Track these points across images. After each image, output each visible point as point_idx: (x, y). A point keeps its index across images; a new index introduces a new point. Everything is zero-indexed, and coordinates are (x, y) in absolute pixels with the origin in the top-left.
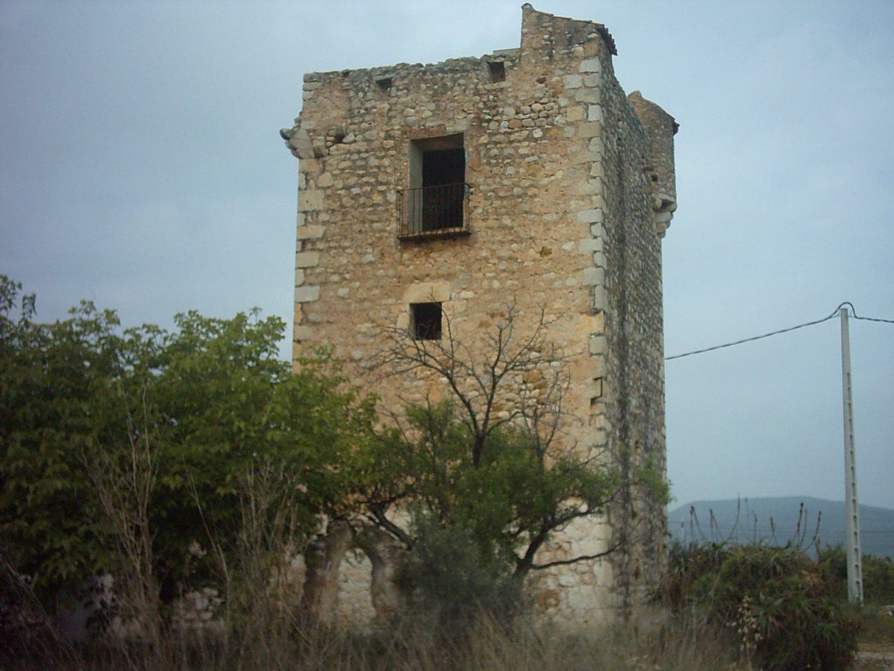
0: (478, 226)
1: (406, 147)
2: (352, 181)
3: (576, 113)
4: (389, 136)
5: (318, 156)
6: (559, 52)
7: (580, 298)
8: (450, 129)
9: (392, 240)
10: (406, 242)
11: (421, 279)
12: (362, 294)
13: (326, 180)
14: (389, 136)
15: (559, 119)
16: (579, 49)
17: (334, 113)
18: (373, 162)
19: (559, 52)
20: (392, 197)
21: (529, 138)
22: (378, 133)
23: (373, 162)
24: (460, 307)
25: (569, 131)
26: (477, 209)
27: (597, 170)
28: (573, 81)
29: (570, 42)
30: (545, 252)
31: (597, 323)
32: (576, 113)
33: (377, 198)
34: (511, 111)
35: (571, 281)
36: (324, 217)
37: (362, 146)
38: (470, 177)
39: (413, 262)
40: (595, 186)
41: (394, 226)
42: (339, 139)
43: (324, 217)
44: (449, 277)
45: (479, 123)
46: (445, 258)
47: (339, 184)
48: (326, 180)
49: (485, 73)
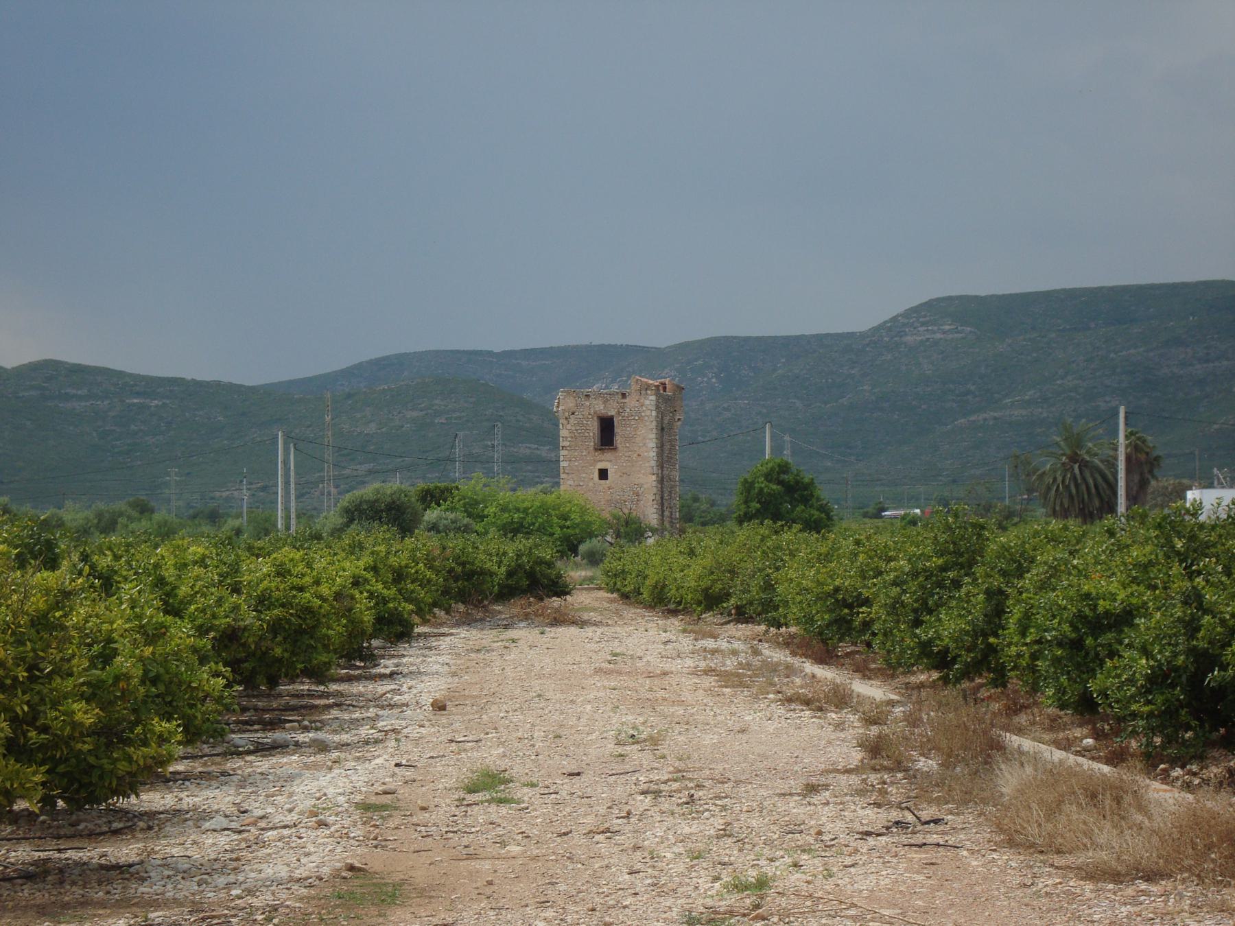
0: (619, 446)
1: (595, 418)
2: (578, 428)
3: (648, 413)
4: (589, 414)
5: (566, 418)
6: (643, 392)
7: (649, 470)
8: (610, 414)
9: (592, 448)
10: (596, 450)
11: (601, 461)
12: (583, 465)
13: (569, 427)
14: (589, 414)
15: (643, 414)
16: (649, 392)
17: (571, 405)
18: (585, 422)
19: (643, 392)
20: (591, 434)
21: (634, 419)
22: (586, 413)
23: (585, 422)
24: (613, 470)
25: (646, 418)
26: (618, 440)
27: (654, 431)
28: (647, 402)
29: (646, 390)
30: (639, 455)
31: (654, 478)
32: (648, 413)
33: (587, 434)
34: (628, 410)
35: (647, 465)
36: (569, 439)
37: (581, 417)
38: (616, 430)
39: (599, 456)
40: (653, 436)
41: (592, 444)
42: (573, 414)
43: (569, 439)
44: (610, 461)
45: (619, 413)
46: (609, 455)
47: (573, 428)
48: (569, 427)
49: (620, 397)
